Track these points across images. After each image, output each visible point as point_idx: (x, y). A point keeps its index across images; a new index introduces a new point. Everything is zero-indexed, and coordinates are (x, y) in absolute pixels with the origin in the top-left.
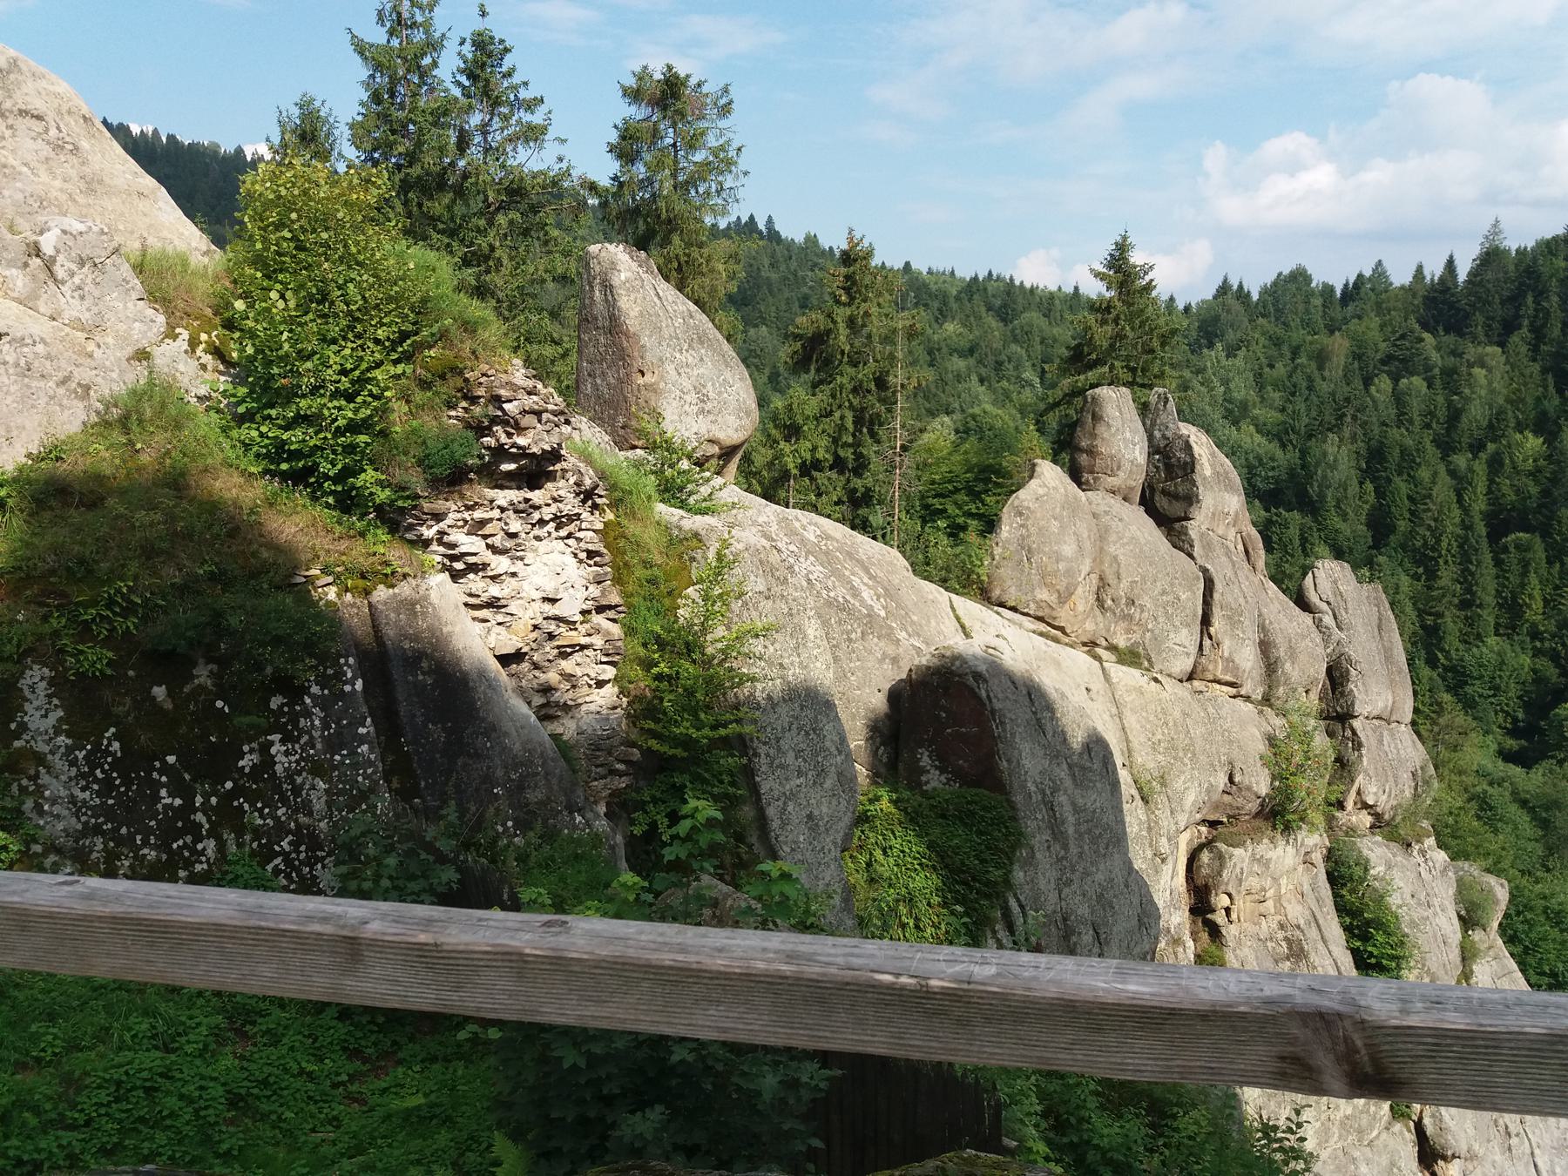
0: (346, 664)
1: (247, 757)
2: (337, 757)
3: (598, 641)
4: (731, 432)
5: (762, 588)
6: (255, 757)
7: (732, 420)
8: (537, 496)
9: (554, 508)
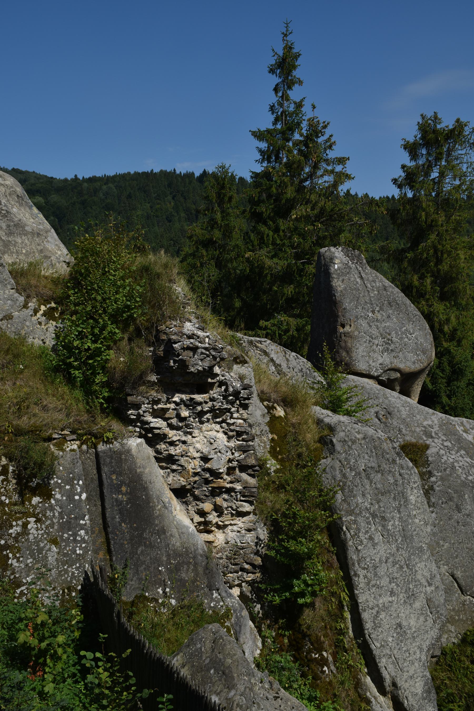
0: (78, 484)
1: (15, 528)
2: (66, 535)
3: (238, 487)
4: (409, 364)
5: (373, 465)
6: (19, 529)
7: (411, 356)
8: (198, 398)
9: (210, 404)
